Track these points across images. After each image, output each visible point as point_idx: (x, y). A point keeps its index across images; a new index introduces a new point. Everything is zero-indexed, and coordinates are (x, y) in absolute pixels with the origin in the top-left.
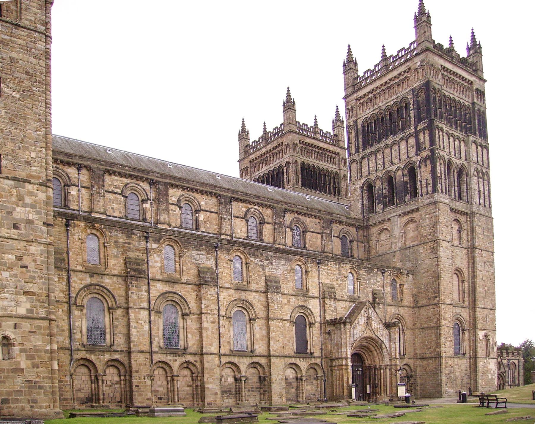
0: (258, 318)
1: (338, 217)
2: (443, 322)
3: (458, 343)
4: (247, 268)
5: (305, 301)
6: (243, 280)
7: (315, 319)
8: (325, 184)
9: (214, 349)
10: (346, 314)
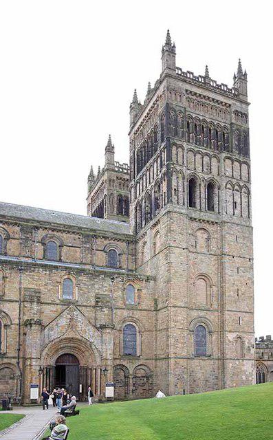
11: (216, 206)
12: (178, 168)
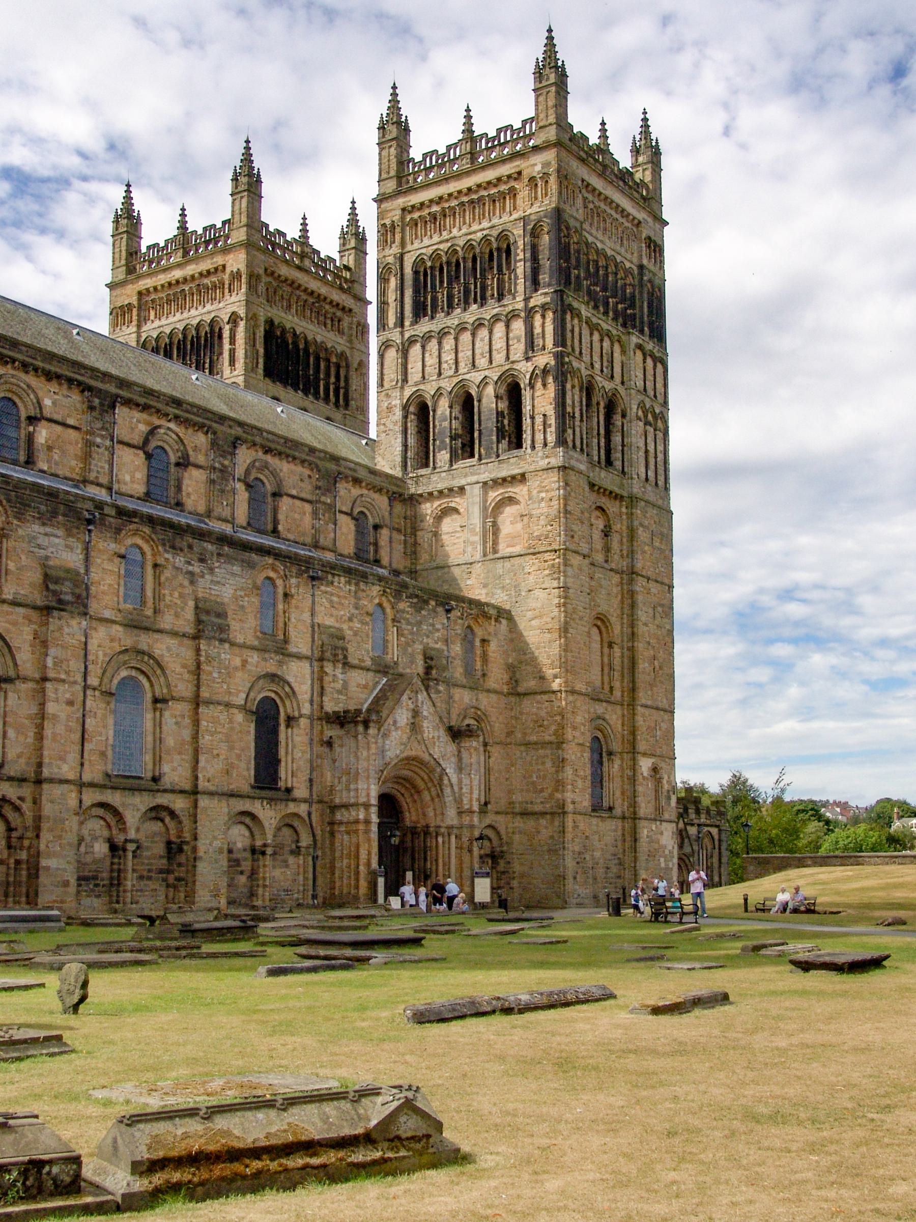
0: (173, 698)
1: (350, 469)
2: (569, 734)
3: (598, 780)
4: (157, 577)
5: (280, 663)
6: (143, 603)
7: (299, 710)
8: (317, 380)
9: (67, 770)
10: (366, 700)
11: (616, 455)
12: (575, 364)
